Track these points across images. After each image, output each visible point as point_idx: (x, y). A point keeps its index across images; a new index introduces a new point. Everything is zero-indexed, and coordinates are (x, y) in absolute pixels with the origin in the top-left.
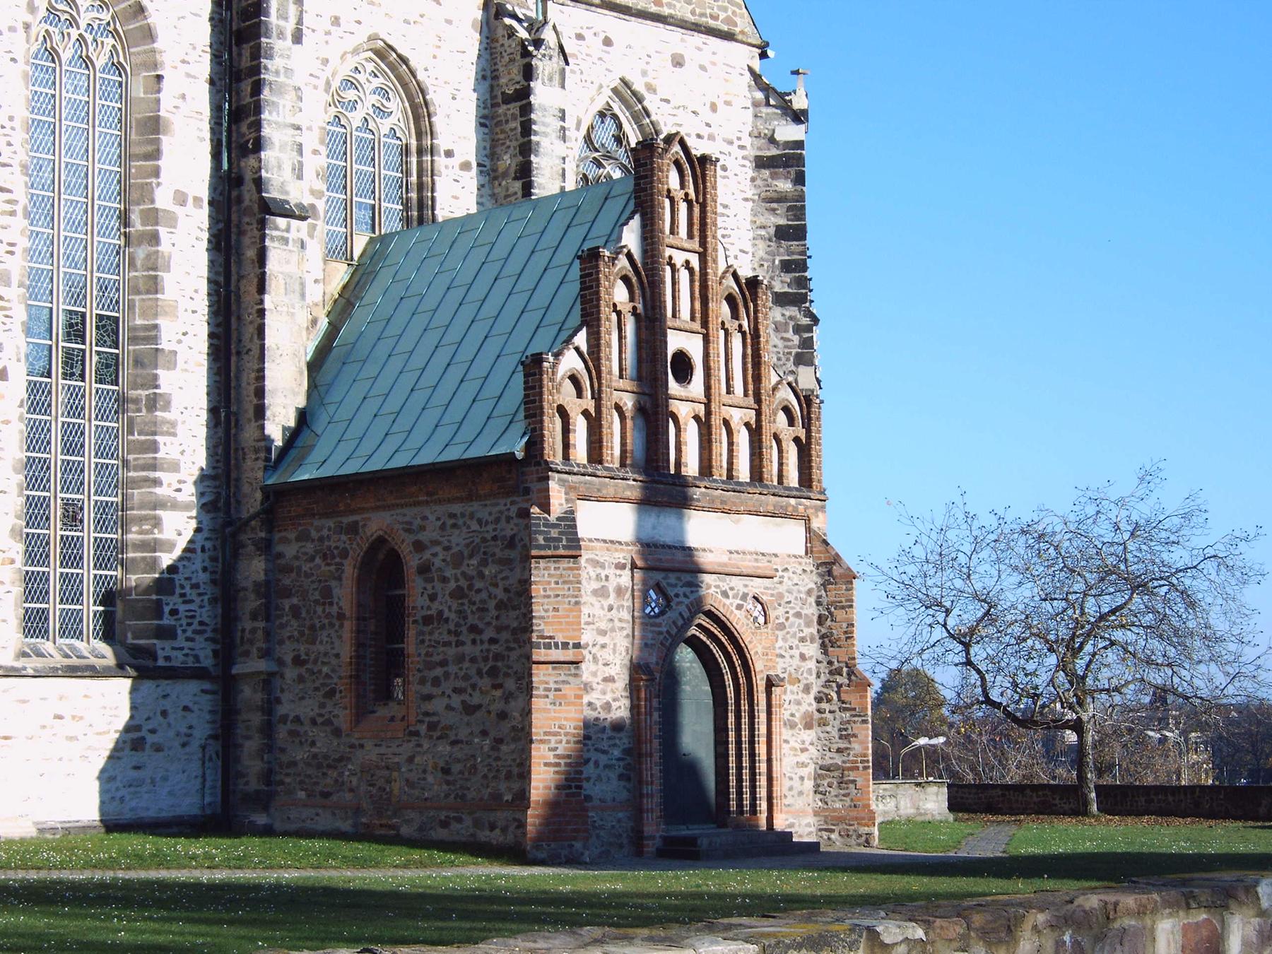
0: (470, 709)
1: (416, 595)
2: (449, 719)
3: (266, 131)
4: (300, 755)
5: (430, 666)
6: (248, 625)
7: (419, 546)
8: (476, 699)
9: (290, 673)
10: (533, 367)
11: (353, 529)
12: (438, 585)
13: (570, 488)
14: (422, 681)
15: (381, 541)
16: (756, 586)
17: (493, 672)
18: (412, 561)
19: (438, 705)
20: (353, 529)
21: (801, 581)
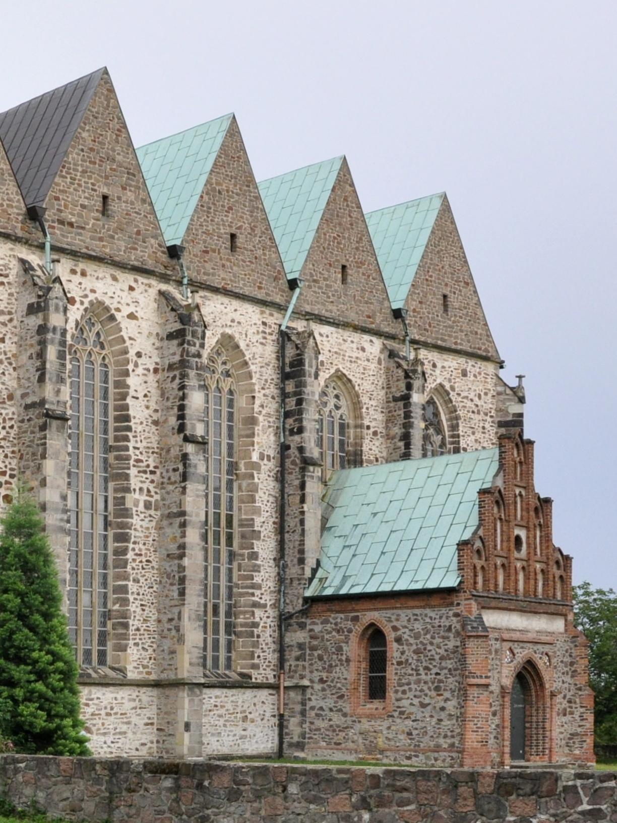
0: (423, 705)
1: (393, 651)
4: (322, 724)
7: (395, 629)
8: (427, 701)
11: (355, 619)
14: (396, 692)
15: (372, 625)
17: (437, 689)
18: (390, 636)
19: (405, 703)
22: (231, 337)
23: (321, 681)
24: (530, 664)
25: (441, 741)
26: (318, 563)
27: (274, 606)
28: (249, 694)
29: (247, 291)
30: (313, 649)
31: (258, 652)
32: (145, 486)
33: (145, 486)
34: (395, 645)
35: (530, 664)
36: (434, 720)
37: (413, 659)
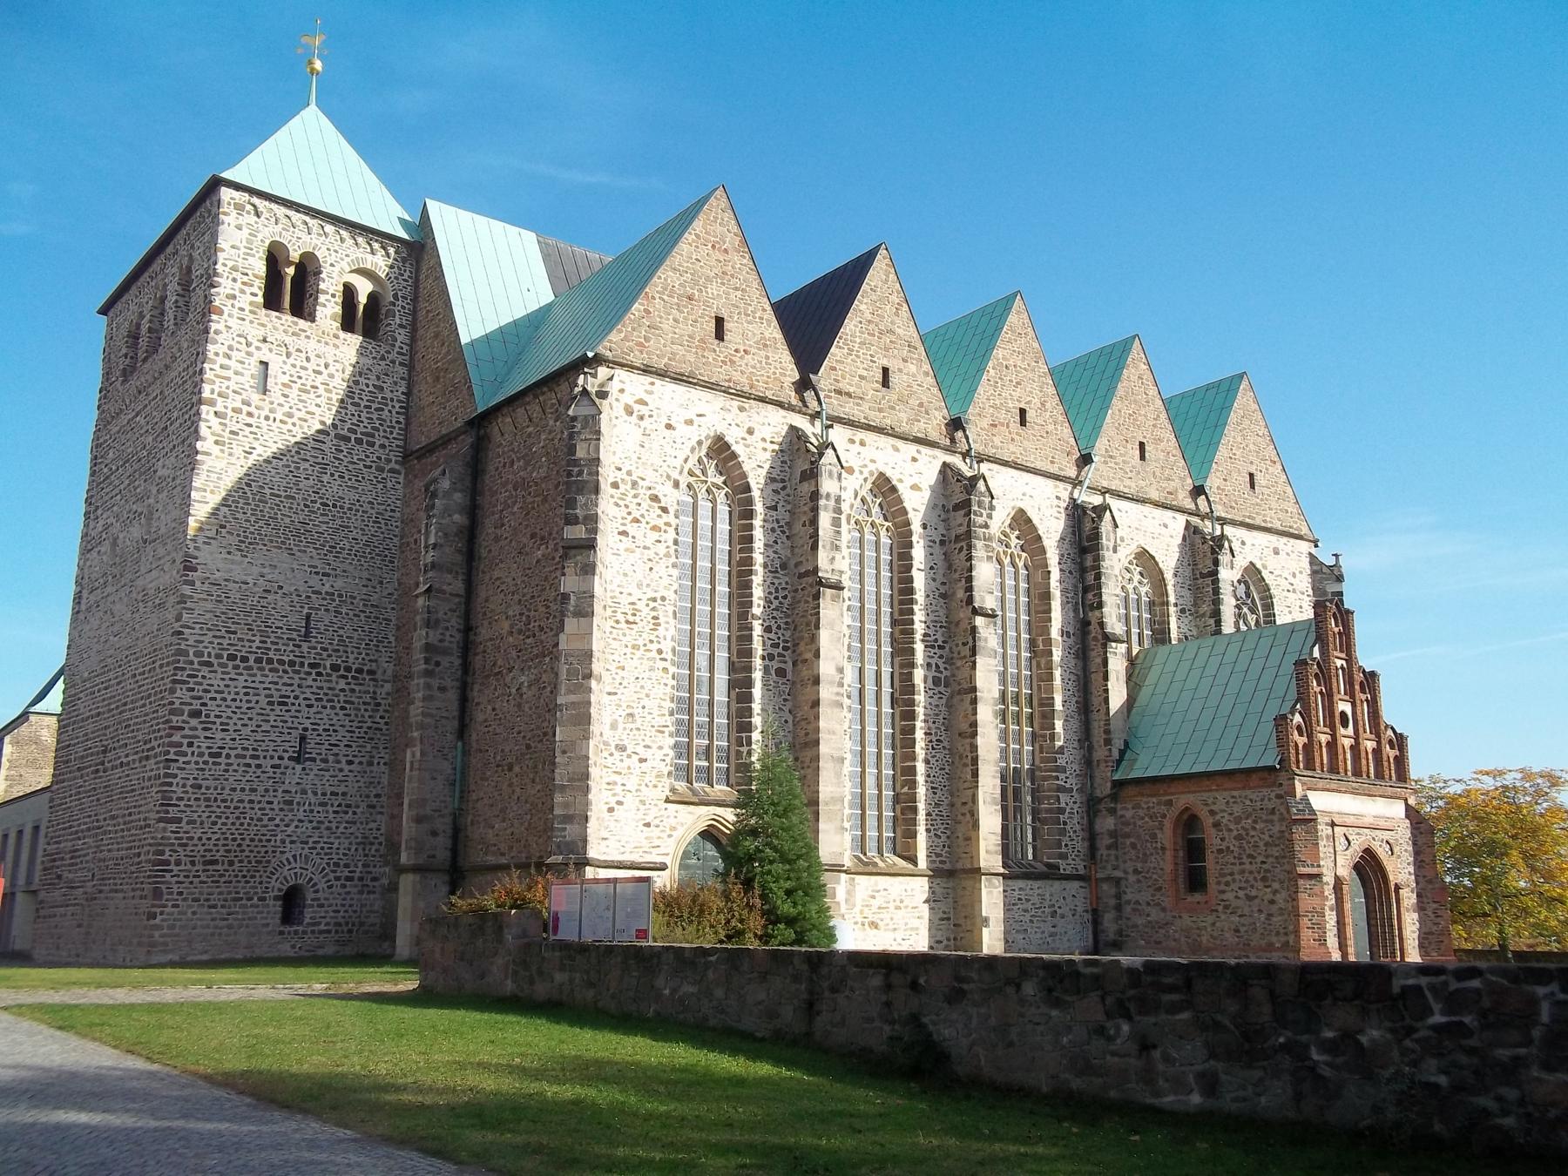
0: (1250, 898)
1: (1212, 839)
2: (1235, 903)
3: (1104, 598)
5: (1224, 875)
6: (1105, 852)
7: (1212, 813)
8: (1254, 893)
10: (1281, 721)
11: (1170, 803)
12: (1226, 834)
13: (1303, 784)
14: (1219, 883)
15: (1187, 809)
16: (1386, 835)
17: (1264, 879)
18: (1208, 821)
19: (1230, 896)
21: (1404, 832)
22: (1021, 512)
24: (1369, 853)
25: (1274, 939)
26: (1126, 744)
27: (1080, 790)
28: (1057, 885)
29: (1039, 465)
31: (1065, 840)
32: (933, 662)
33: (933, 662)
34: (1213, 831)
35: (1369, 853)
36: (1263, 917)
37: (1233, 845)
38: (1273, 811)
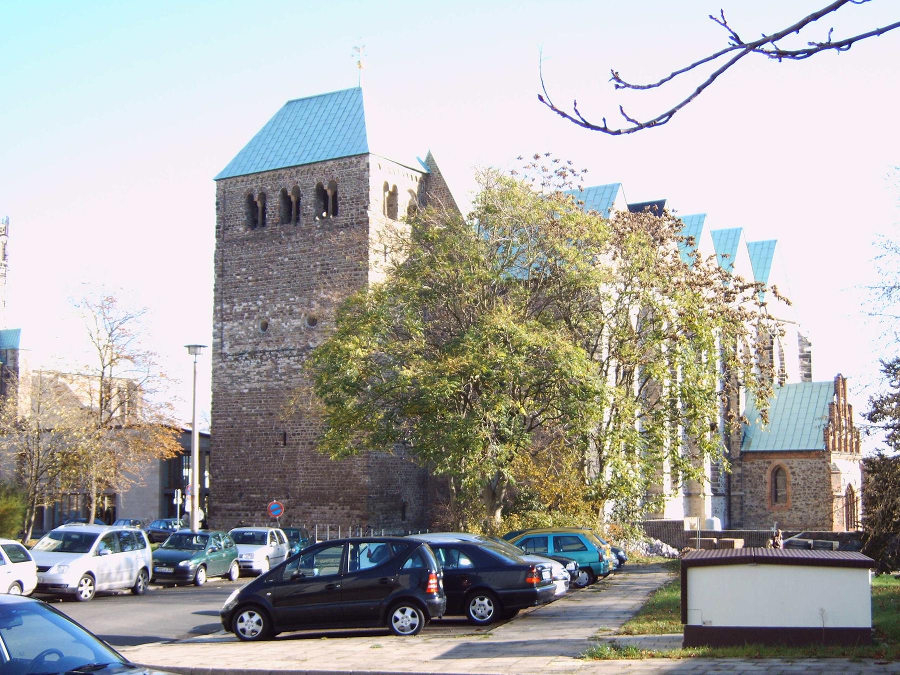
2: (800, 507)
7: (791, 468)
9: (749, 495)
11: (769, 463)
17: (815, 497)
20: (769, 463)
23: (751, 492)
30: (747, 476)
34: (792, 476)
37: (801, 483)
38: (821, 469)
